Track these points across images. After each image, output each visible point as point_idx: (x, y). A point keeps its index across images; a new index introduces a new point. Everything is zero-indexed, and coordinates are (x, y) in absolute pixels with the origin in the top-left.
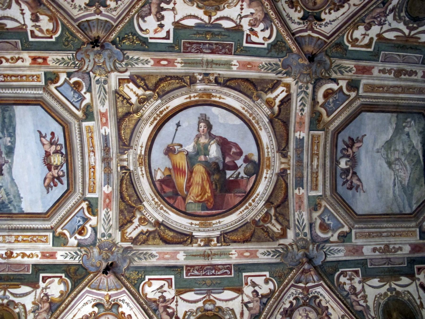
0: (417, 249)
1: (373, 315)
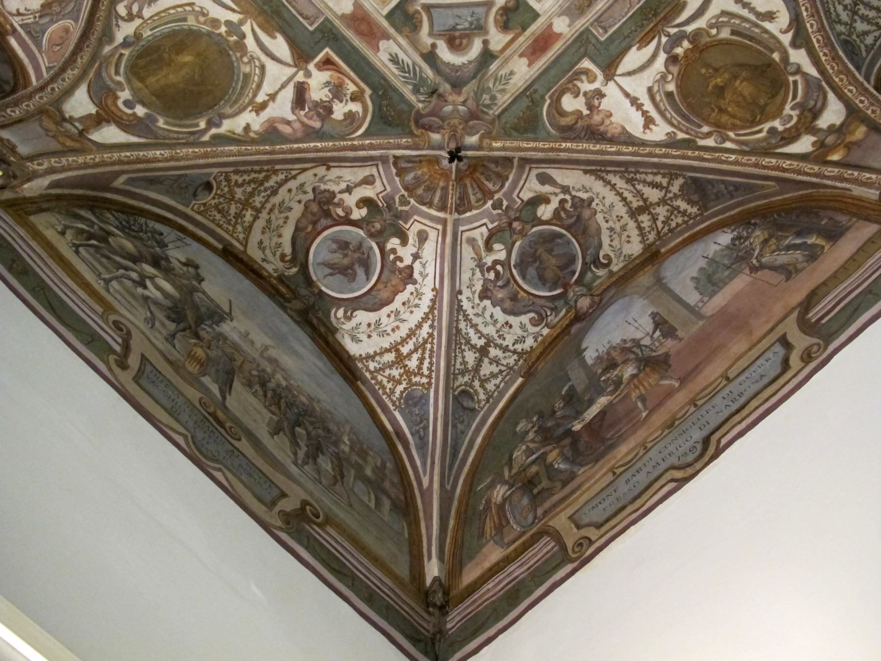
0: (363, 27)
1: (147, 13)
